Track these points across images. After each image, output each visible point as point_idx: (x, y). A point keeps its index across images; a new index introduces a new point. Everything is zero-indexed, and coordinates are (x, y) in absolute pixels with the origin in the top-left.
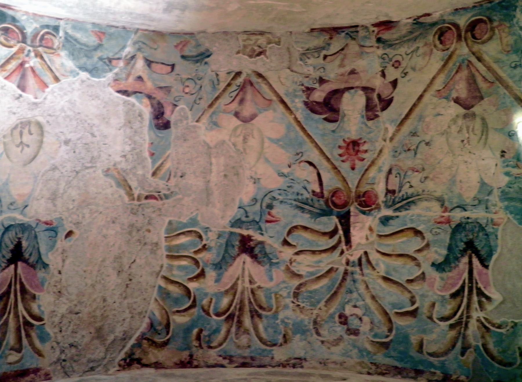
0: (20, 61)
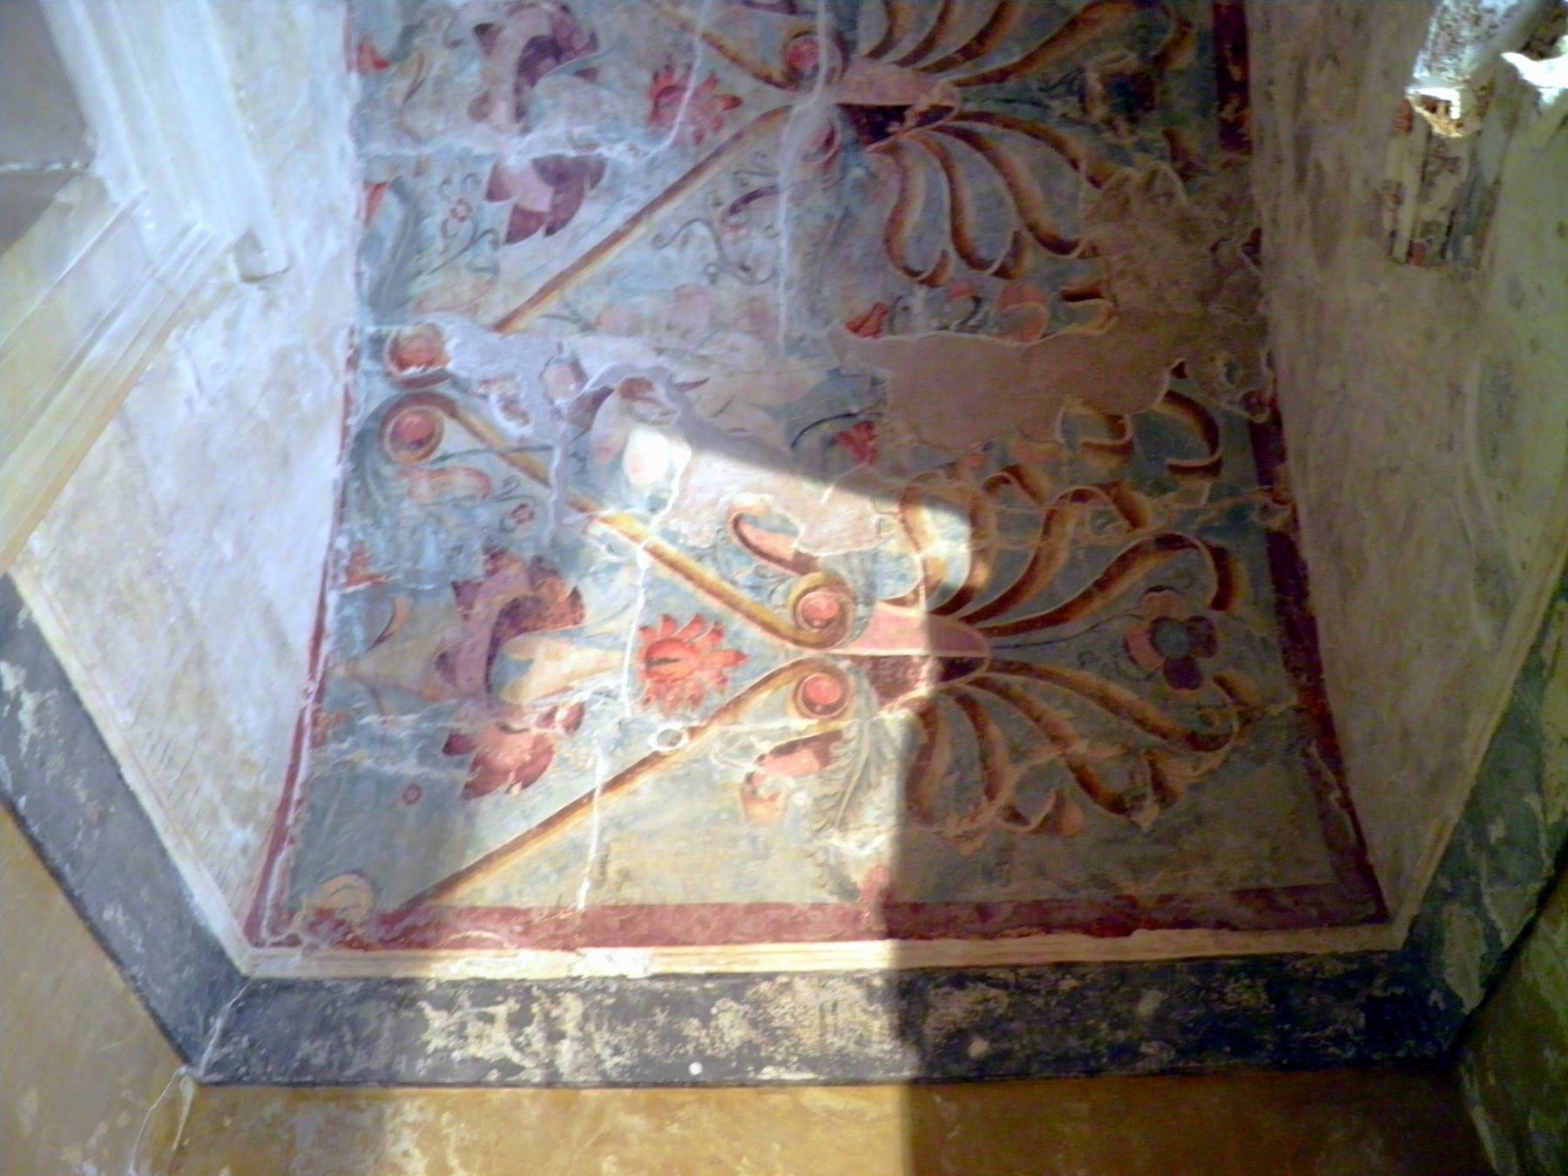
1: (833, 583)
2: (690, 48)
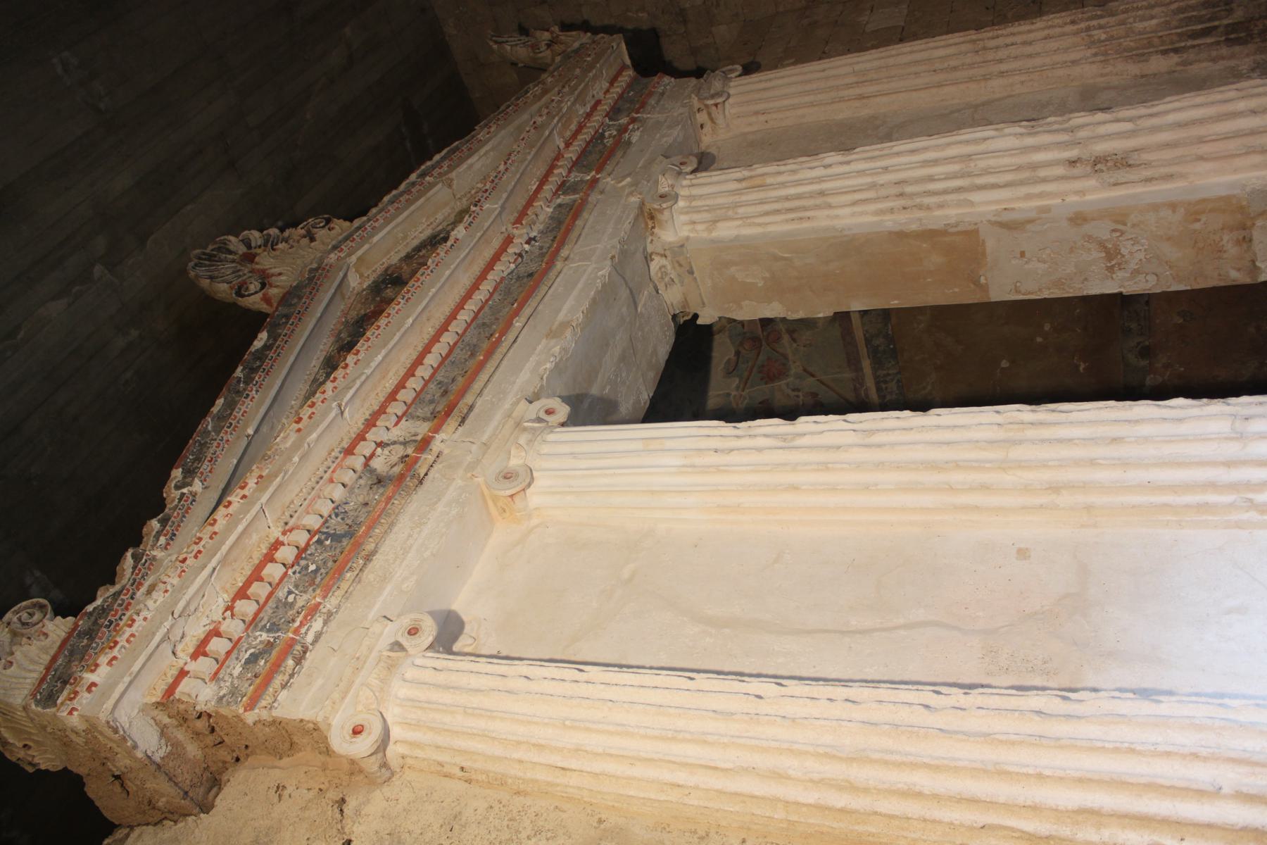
1: (741, 344)
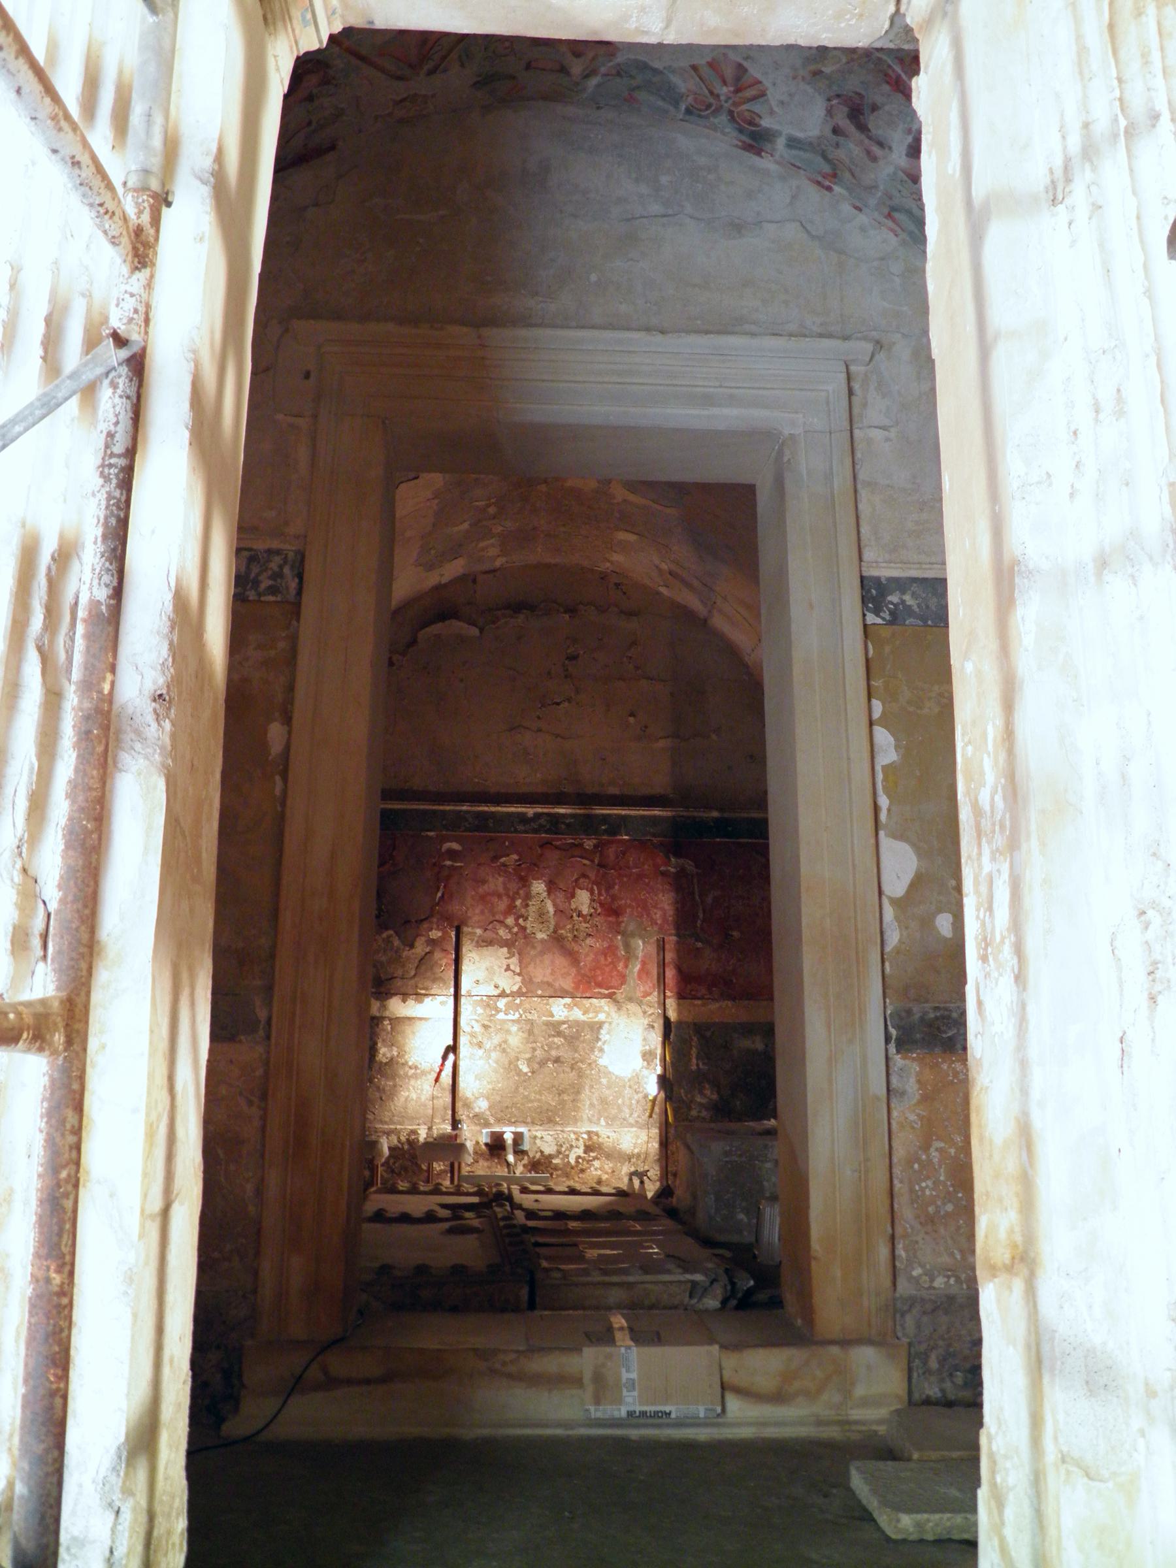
0: (740, 95)
2: (879, 59)
